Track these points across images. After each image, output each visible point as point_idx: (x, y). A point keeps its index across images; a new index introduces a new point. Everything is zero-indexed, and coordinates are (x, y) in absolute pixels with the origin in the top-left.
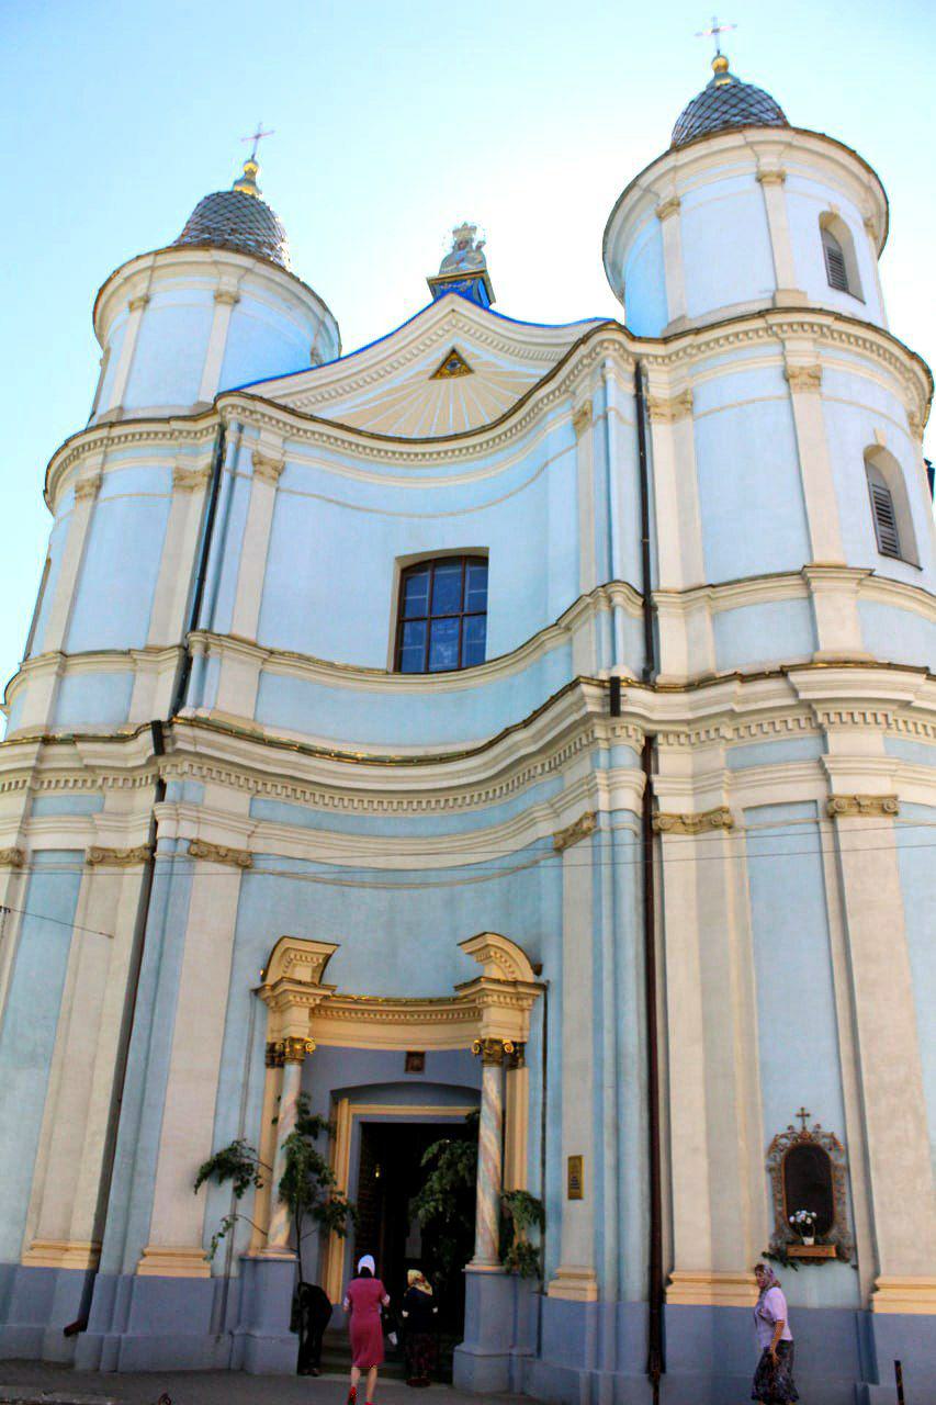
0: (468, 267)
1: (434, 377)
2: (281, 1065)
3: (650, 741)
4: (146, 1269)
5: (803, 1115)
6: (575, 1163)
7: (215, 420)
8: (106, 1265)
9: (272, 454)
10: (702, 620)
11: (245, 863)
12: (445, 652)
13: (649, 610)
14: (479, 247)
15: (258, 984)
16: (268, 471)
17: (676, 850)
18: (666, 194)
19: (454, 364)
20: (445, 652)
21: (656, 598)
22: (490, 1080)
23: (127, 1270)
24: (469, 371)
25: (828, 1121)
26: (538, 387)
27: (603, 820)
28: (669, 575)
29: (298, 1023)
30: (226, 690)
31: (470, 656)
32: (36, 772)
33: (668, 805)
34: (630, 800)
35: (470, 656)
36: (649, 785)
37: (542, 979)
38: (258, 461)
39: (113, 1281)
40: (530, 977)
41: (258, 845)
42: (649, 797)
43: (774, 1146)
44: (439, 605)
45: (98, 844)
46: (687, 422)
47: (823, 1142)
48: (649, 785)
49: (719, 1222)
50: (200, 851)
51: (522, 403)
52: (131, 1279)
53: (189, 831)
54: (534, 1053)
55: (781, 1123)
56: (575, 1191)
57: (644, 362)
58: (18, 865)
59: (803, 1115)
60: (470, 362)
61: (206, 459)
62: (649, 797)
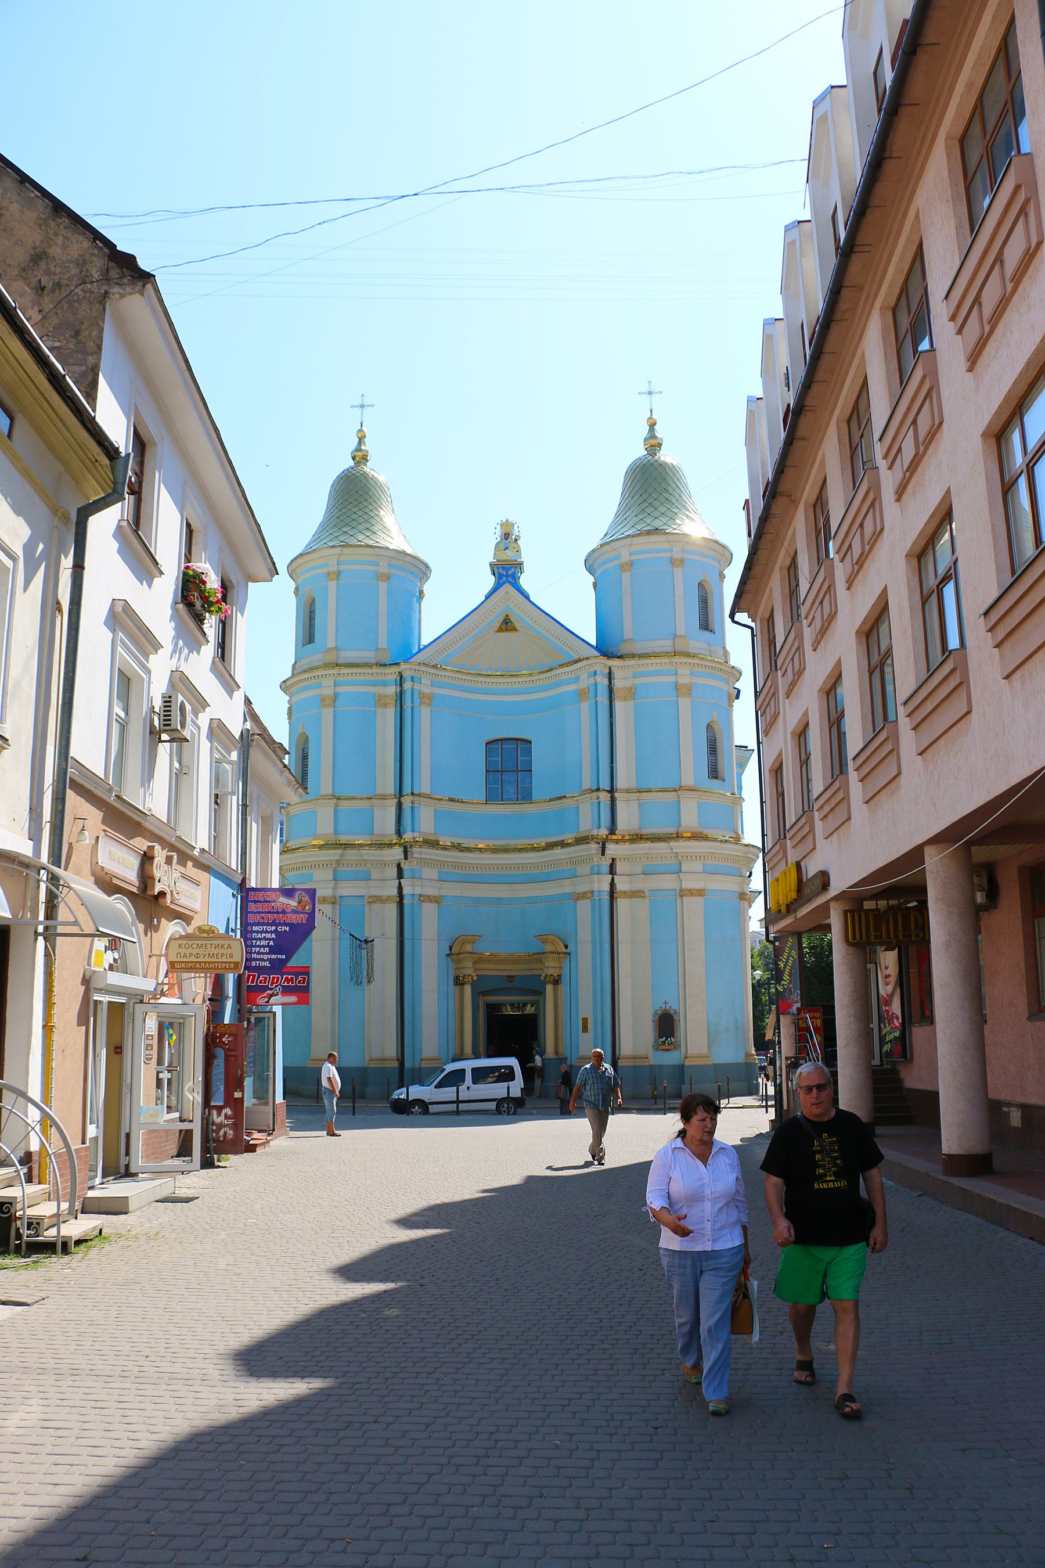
0: (510, 555)
1: (498, 631)
2: (462, 984)
3: (613, 860)
4: (424, 1064)
5: (666, 1003)
6: (585, 1021)
7: (395, 669)
8: (408, 1064)
9: (427, 690)
10: (634, 806)
11: (437, 900)
12: (510, 790)
13: (613, 800)
14: (516, 540)
15: (448, 952)
16: (426, 700)
17: (622, 904)
18: (625, 558)
19: (507, 625)
20: (510, 790)
21: (616, 795)
22: (549, 988)
23: (417, 1066)
24: (516, 630)
25: (673, 1005)
26: (561, 666)
27: (596, 894)
28: (621, 783)
29: (469, 969)
30: (425, 821)
31: (525, 796)
32: (338, 862)
33: (621, 885)
34: (606, 887)
35: (525, 796)
36: (613, 879)
37: (568, 951)
38: (422, 695)
39: (413, 1069)
40: (564, 950)
41: (443, 893)
42: (612, 884)
43: (656, 1013)
44: (508, 765)
45: (372, 893)
46: (631, 703)
47: (672, 1012)
48: (613, 879)
49: (636, 1039)
50: (423, 898)
51: (551, 670)
52: (420, 1069)
53: (418, 891)
54: (565, 979)
55: (659, 1006)
56: (585, 1029)
57: (613, 669)
58: (333, 903)
59: (666, 1003)
60: (516, 624)
61: (392, 690)
62: (612, 884)
